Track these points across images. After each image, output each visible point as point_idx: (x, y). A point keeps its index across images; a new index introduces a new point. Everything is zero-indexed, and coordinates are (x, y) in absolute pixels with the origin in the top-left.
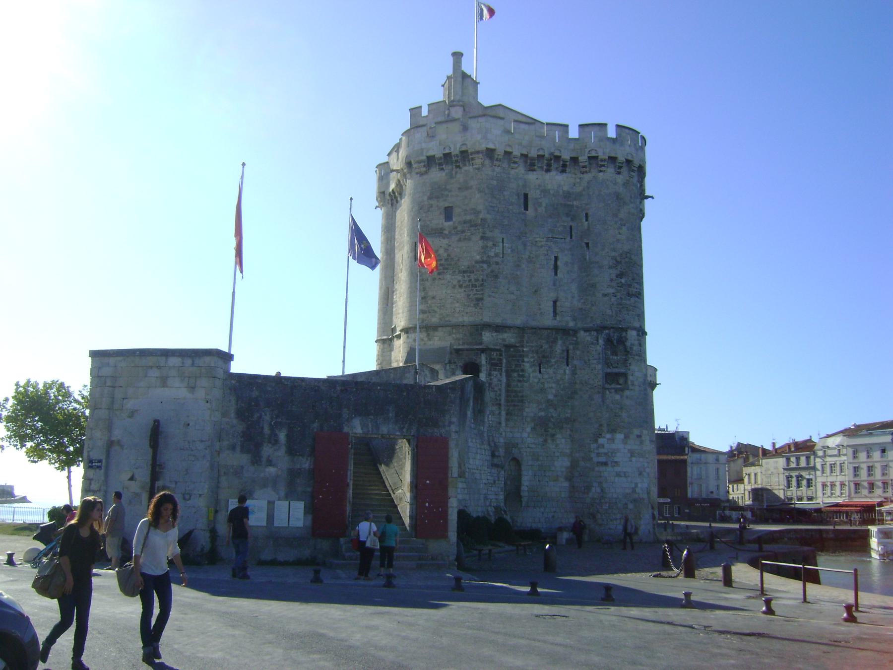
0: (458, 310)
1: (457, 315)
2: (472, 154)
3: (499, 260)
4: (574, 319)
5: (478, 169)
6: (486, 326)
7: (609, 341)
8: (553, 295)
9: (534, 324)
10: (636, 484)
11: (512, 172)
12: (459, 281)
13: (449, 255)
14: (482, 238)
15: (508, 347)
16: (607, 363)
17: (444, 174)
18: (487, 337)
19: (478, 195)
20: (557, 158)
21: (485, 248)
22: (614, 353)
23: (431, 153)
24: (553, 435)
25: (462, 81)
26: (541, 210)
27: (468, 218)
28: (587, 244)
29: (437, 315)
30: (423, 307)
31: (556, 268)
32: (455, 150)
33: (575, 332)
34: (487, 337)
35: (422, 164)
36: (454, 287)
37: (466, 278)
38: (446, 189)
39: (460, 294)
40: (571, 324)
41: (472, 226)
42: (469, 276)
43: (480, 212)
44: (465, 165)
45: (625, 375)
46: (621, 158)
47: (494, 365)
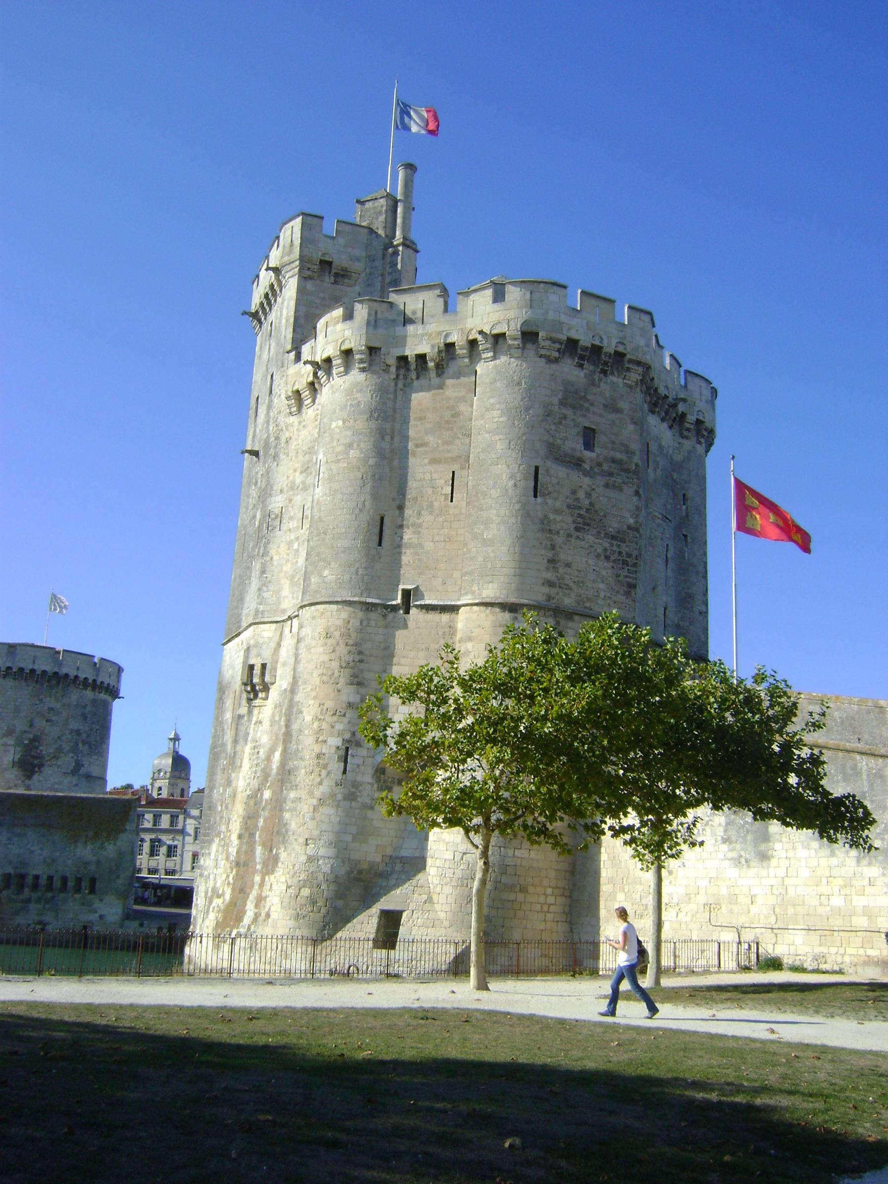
0: (602, 594)
1: (601, 602)
2: (630, 361)
5: (631, 387)
8: (664, 598)
12: (605, 550)
13: (591, 504)
14: (637, 493)
17: (582, 374)
19: (631, 427)
23: (574, 335)
26: (659, 472)
27: (618, 456)
28: (685, 536)
29: (573, 595)
30: (550, 575)
32: (610, 346)
35: (557, 346)
36: (598, 556)
37: (615, 548)
38: (584, 398)
39: (606, 570)
41: (622, 470)
42: (619, 546)
43: (633, 453)
44: (612, 373)
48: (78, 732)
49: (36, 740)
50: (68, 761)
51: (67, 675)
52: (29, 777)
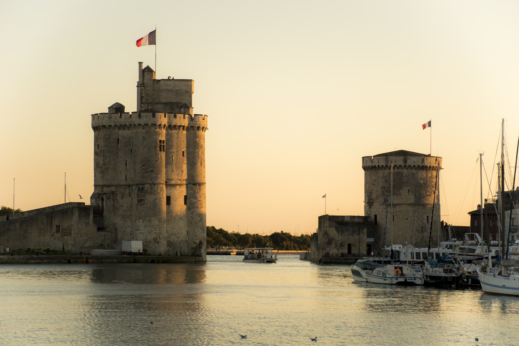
3: (109, 163)
4: (132, 181)
6: (104, 186)
7: (139, 189)
9: (120, 184)
10: (147, 237)
11: (113, 131)
14: (103, 156)
15: (113, 192)
16: (138, 197)
18: (105, 189)
20: (125, 125)
21: (104, 160)
22: (141, 193)
24: (126, 221)
25: (146, 72)
31: (126, 164)
33: (132, 186)
34: (105, 189)
40: (131, 183)
45: (144, 200)
46: (143, 124)
47: (108, 198)
48: (384, 187)
49: (371, 193)
50: (381, 199)
51: (375, 166)
52: (370, 207)
